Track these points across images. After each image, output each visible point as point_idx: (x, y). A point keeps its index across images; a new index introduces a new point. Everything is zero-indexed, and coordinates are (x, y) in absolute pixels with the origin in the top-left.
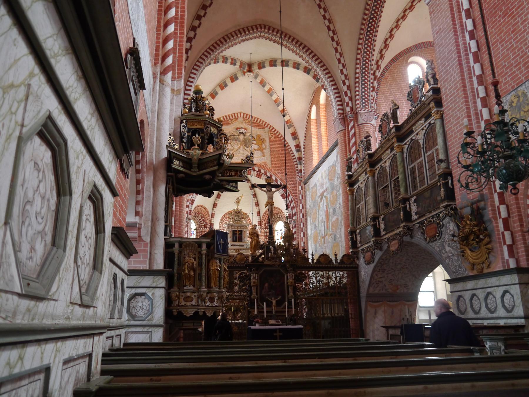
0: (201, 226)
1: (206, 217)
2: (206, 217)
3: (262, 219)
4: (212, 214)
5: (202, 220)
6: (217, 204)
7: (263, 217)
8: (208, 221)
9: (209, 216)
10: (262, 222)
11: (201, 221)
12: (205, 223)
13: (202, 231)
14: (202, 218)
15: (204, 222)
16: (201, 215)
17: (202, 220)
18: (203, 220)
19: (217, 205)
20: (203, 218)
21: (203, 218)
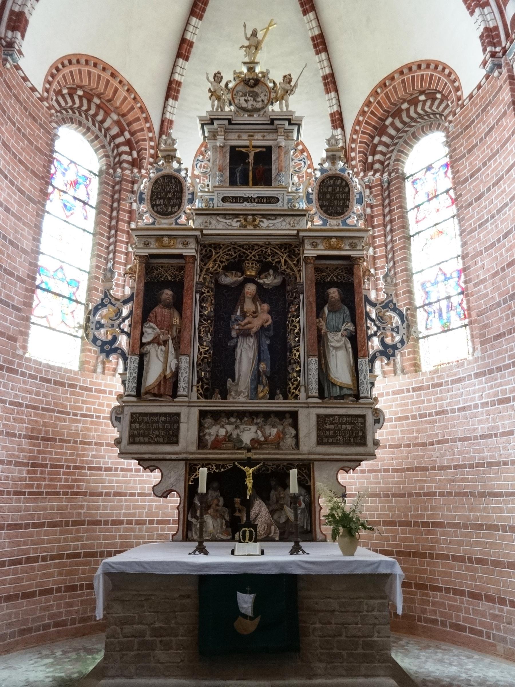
0: (120, 163)
1: (136, 126)
2: (136, 126)
3: (353, 141)
4: (162, 122)
5: (121, 140)
6: (179, 84)
7: (355, 132)
8: (147, 144)
9: (150, 129)
10: (353, 150)
11: (118, 146)
12: (135, 154)
13: (123, 180)
14: (121, 133)
15: (132, 149)
16: (115, 117)
17: (121, 140)
18: (128, 143)
19: (182, 90)
20: (127, 135)
21: (127, 135)
